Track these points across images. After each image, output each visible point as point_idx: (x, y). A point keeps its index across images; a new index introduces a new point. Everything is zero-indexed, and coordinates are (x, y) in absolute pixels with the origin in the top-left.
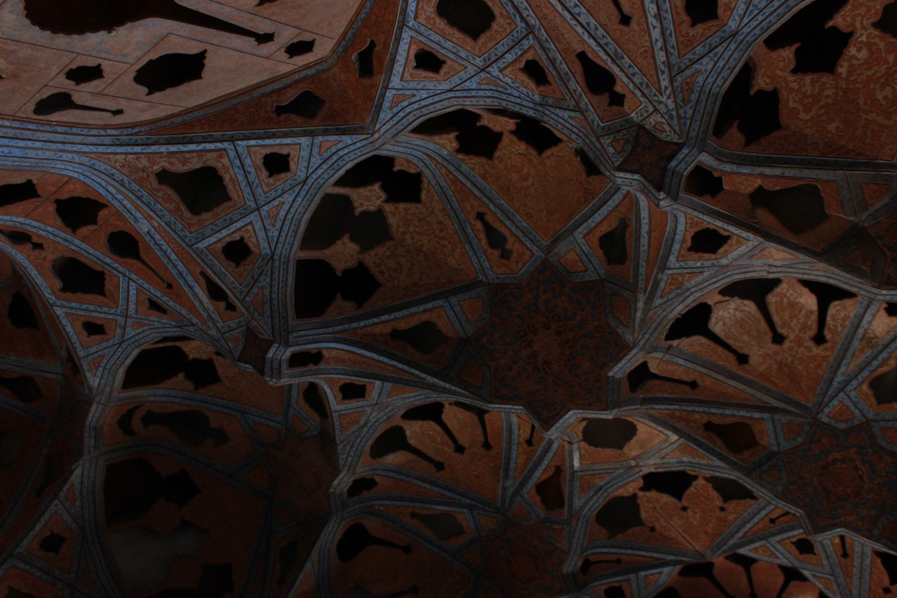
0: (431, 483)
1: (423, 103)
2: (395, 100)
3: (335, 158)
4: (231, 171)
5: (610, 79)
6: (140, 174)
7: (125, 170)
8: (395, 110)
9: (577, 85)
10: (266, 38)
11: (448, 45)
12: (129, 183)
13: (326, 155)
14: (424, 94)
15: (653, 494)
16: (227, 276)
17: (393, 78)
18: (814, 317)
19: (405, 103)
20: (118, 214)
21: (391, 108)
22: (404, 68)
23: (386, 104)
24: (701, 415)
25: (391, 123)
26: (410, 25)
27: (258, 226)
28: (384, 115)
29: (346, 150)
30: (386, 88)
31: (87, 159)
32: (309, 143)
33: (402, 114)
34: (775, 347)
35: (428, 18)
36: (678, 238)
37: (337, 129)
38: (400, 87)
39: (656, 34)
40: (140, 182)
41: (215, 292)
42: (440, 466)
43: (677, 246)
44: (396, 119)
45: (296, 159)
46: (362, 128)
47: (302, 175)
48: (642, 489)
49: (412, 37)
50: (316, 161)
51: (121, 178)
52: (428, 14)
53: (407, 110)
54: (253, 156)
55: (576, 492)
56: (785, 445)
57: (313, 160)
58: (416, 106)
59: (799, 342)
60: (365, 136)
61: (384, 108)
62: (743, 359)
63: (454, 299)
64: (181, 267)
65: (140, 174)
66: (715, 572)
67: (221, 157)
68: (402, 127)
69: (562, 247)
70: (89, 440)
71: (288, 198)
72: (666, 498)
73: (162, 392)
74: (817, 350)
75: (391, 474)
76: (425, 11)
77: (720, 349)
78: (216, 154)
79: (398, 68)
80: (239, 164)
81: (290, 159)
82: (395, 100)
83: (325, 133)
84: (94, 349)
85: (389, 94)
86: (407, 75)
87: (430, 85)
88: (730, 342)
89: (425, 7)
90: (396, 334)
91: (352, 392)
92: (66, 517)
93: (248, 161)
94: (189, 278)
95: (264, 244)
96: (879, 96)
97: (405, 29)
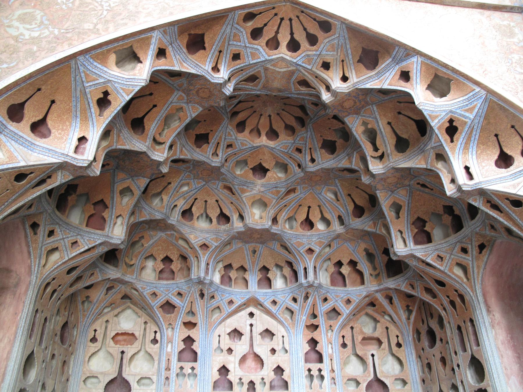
0: (325, 205)
5: (200, 295)
9: (206, 297)
10: (251, 325)
11: (224, 306)
15: (267, 167)
16: (300, 299)
18: (195, 204)
20: (306, 322)
23: (245, 299)
24: (233, 199)
27: (288, 299)
28: (248, 297)
34: (207, 200)
36: (209, 252)
39: (188, 298)
40: (295, 324)
41: (307, 297)
42: (319, 206)
43: (211, 250)
48: (268, 170)
50: (268, 297)
55: (281, 193)
56: (217, 182)
59: (201, 200)
62: (217, 201)
63: (273, 248)
64: (307, 307)
66: (268, 129)
69: (240, 246)
70: (382, 287)
71: (279, 296)
72: (264, 165)
73: (364, 270)
74: (198, 197)
75: (333, 214)
77: (221, 206)
79: (237, 305)
84: (355, 299)
88: (218, 206)
90: (290, 253)
91: (310, 251)
92: (404, 285)
93: (277, 309)
94: (308, 304)
95: (290, 296)
96: (161, 248)
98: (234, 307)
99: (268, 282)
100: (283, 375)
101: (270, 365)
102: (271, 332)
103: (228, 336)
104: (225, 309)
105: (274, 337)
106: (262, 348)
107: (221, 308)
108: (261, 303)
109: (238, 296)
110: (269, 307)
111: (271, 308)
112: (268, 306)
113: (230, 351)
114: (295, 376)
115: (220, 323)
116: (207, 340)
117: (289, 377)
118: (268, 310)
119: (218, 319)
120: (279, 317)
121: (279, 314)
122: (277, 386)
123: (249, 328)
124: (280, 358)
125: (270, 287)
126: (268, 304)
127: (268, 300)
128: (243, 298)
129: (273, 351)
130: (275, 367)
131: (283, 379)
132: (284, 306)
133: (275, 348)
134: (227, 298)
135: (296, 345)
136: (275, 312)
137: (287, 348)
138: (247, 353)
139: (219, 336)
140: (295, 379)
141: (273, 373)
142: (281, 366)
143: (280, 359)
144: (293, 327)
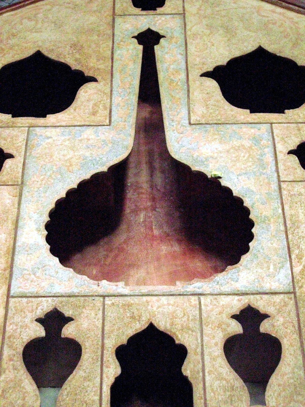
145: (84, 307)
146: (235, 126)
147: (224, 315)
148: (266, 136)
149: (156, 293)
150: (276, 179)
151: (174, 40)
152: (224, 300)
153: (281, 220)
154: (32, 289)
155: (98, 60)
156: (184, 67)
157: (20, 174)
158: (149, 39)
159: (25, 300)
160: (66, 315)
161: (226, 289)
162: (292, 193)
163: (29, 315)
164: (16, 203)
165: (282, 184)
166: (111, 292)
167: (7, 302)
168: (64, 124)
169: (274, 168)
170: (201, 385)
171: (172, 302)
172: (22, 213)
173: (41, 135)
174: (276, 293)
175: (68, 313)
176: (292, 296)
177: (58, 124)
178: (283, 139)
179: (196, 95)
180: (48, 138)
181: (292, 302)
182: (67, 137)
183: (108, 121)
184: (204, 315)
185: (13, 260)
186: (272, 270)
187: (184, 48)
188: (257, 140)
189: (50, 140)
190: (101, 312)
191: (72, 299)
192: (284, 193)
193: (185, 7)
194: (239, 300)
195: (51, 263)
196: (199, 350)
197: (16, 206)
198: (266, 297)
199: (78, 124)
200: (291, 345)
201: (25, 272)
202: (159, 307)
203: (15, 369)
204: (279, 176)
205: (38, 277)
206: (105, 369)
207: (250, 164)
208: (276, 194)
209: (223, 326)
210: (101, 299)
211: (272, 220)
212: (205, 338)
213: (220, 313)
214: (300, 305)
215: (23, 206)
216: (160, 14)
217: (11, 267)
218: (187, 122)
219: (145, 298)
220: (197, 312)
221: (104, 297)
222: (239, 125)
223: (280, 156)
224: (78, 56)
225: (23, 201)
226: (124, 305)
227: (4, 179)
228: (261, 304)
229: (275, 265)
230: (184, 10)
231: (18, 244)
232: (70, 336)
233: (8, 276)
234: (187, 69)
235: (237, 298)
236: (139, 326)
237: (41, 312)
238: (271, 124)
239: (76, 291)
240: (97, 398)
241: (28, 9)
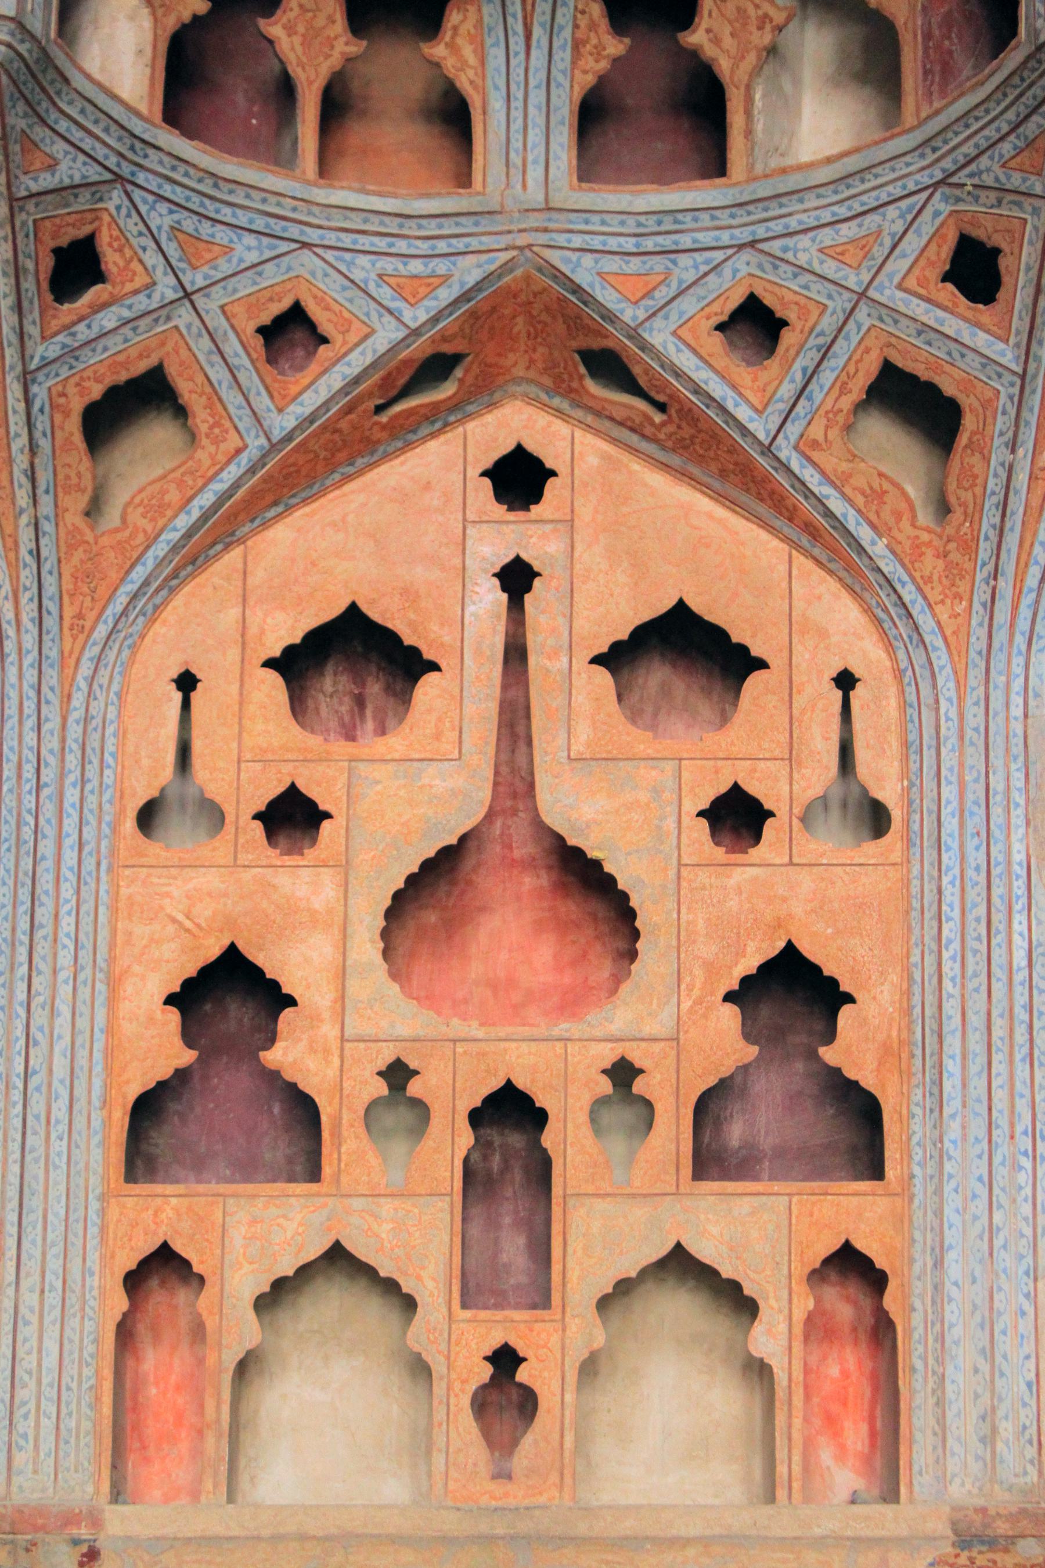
1: (381, 244)
2: (423, 291)
3: (649, 244)
4: (828, 405)
6: (955, 556)
7: (963, 587)
8: (441, 267)
12: (984, 564)
13: (659, 264)
14: (363, 268)
17: (382, 349)
19: (416, 267)
21: (446, 278)
22: (346, 354)
23: (445, 295)
25: (474, 243)
26: (263, 441)
29: (613, 243)
30: (416, 333)
31: (971, 673)
32: (658, 322)
33: (442, 246)
35: (216, 442)
37: (585, 303)
38: (387, 318)
44: (459, 244)
45: (716, 307)
46: (540, 270)
47: (744, 263)
49: (280, 410)
50: (686, 268)
51: (984, 587)
52: (212, 449)
53: (424, 247)
54: (770, 389)
57: (690, 276)
58: (401, 246)
60: (547, 254)
61: (455, 292)
65: (955, 556)
67: (815, 444)
68: (463, 220)
76: (212, 457)
78: (815, 455)
79: (357, 361)
80: (802, 402)
81: (724, 318)
82: (423, 291)
83: (610, 317)
85: (417, 316)
86: (352, 338)
87: (332, 286)
89: (207, 462)
93: (787, 390)
97: (277, 435)
98: (322, 385)
99: (702, 116)
100: (830, 1035)
101: (707, 950)
102: (717, 635)
103: (273, 677)
104: (232, 398)
105: (755, 681)
106: (624, 786)
107: (185, 388)
108: (618, 339)
109: (363, 268)
110: (702, 375)
111: (717, 389)
112: (686, 361)
113: (292, 817)
114: (953, 1044)
115: (193, 556)
116: (52, 713)
117: (893, 1054)
118: (689, 415)
119: (159, 510)
120: (811, 477)
121: (806, 447)
122: (780, 1153)
123: (489, 598)
124: (806, 881)
125: (716, 166)
126: (681, 344)
127: (689, 305)
128: (412, 290)
129: (737, 816)
130: (750, 963)
131: (837, 1072)
132: (854, 365)
133: (753, 788)
134: (249, 278)
135: (974, 758)
136: (760, 428)
137: (888, 794)
138: (463, 839)
139: (187, 682)
140: (952, 1066)
141: (730, 1016)
142: (808, 949)
143: (802, 890)
144: (954, 572)
145: (432, 1056)
146: (630, 763)
147: (593, 1070)
148: (670, 783)
149: (515, 1037)
150: (675, 861)
151: (554, 583)
152: (596, 1049)
153: (675, 930)
154: (368, 1030)
155: (442, 625)
156: (566, 645)
157: (343, 848)
158: (517, 578)
159: (362, 1045)
160: (411, 1067)
161: (598, 1033)
162: (694, 885)
163: (369, 1066)
164: (341, 896)
165: (682, 869)
166: (463, 1036)
167: (342, 1049)
168: (397, 756)
169: (675, 842)
170: (561, 1161)
171: (533, 1050)
172: (351, 913)
173: (366, 778)
174: (655, 1040)
175: (413, 1065)
176: (675, 1043)
177: (389, 757)
178: (692, 789)
179: (580, 699)
180: (377, 782)
181: (674, 1052)
182: (402, 782)
183: (456, 752)
184: (570, 1069)
185: (344, 986)
186: (654, 1006)
187: (567, 602)
188: (657, 791)
189: (379, 787)
190: (451, 1064)
191: (418, 1045)
192: (684, 884)
193: (576, 504)
194: (612, 1049)
195: (391, 993)
196: (561, 1115)
197: (342, 902)
198: (643, 1044)
199: (417, 756)
200: (666, 1111)
201: (360, 1005)
202: (518, 1057)
203: (357, 1137)
204: (679, 855)
205: (376, 1013)
206: (457, 1139)
207: (644, 835)
208: (672, 887)
209: (592, 1085)
210: (451, 1045)
211: (663, 930)
212: (570, 1101)
213: (589, 1067)
214: (682, 1057)
215: (351, 902)
216: (537, 521)
217: (343, 997)
218: (566, 754)
219: (503, 1045)
220: (563, 1065)
221: (455, 1041)
222: (635, 763)
223: (686, 821)
224: (412, 616)
225: (350, 895)
226: (478, 1054)
227: (322, 856)
228: (637, 1056)
229: (659, 999)
230: (572, 511)
231: (349, 962)
232: (416, 1096)
233: (340, 1010)
234: (571, 646)
235: (610, 1045)
236: (495, 1084)
237: (382, 1064)
238: (680, 760)
239: (421, 1033)
240: (448, 1174)
241: (331, 500)
